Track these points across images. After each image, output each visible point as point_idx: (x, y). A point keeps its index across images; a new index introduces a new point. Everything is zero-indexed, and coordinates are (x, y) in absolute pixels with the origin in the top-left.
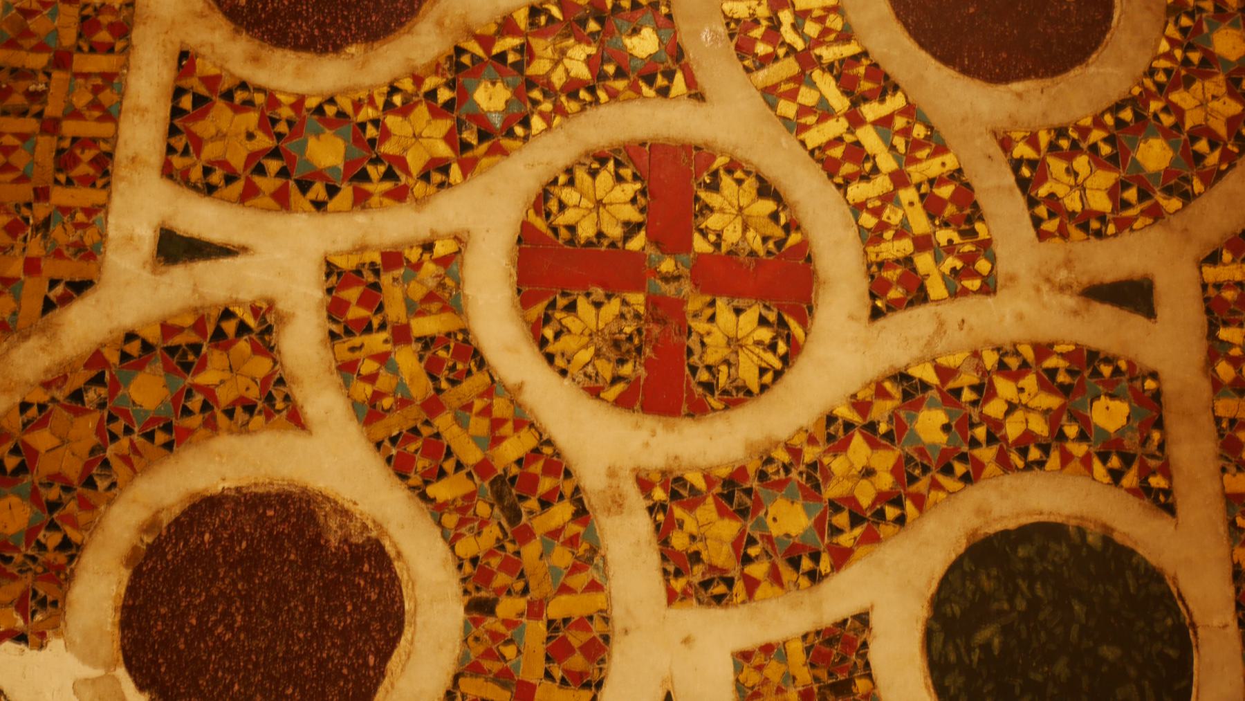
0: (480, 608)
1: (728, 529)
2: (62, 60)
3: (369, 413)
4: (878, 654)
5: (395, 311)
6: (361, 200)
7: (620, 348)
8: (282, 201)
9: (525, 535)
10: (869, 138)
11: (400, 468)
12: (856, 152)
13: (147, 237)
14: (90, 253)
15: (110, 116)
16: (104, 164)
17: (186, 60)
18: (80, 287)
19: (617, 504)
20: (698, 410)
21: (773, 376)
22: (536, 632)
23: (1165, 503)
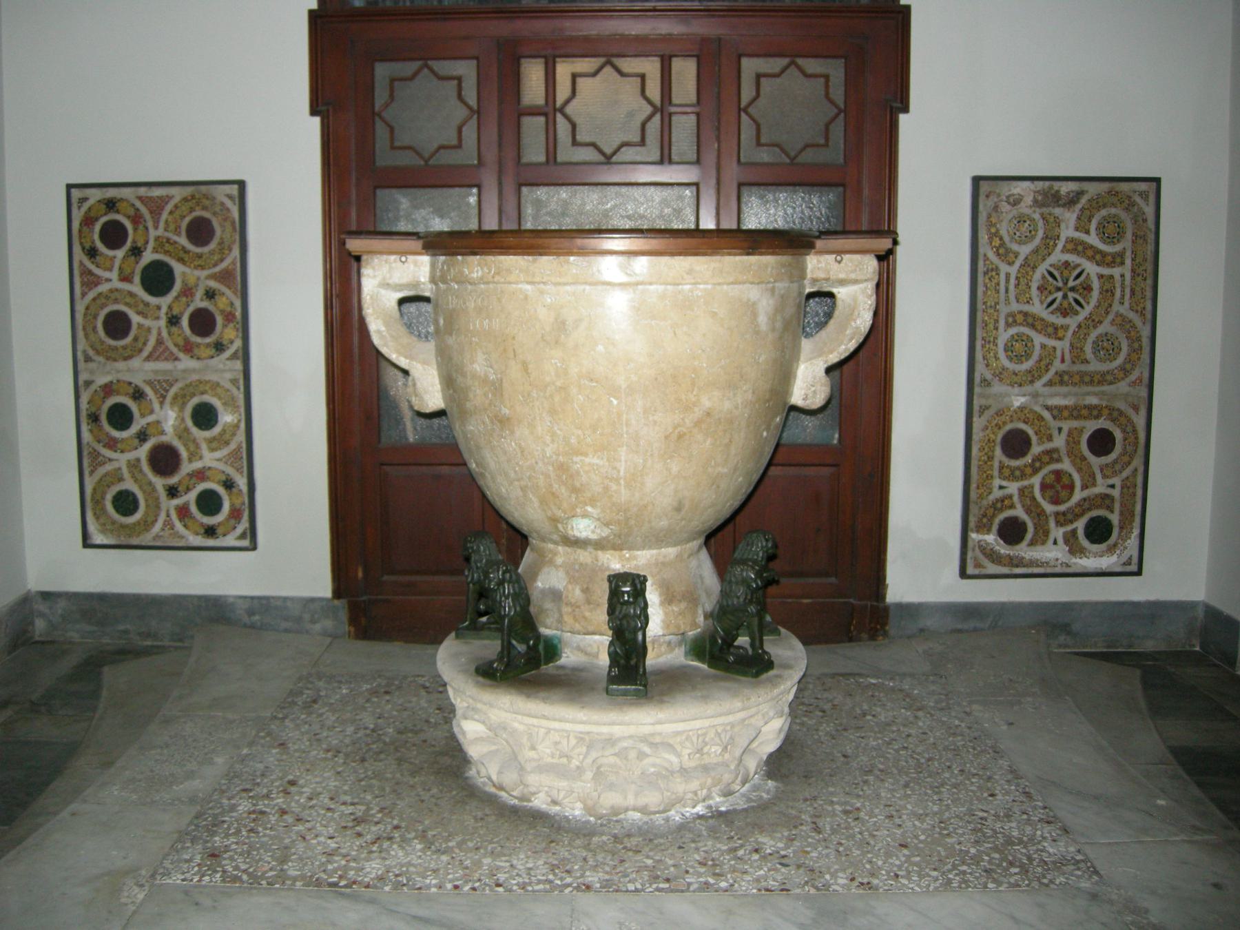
0: (1036, 528)
1: (1063, 518)
2: (986, 463)
3: (1023, 506)
4: (1079, 531)
5: (1026, 494)
6: (1022, 480)
7: (1051, 497)
8: (1013, 480)
9: (1040, 519)
10: (1082, 466)
11: (1027, 513)
12: (1081, 469)
13: (997, 486)
14: (991, 489)
15: (992, 470)
16: (992, 477)
17: (1000, 462)
18: (990, 493)
19: (1050, 515)
20: (1060, 504)
21: (1069, 499)
22: (1041, 531)
23: (1112, 512)
